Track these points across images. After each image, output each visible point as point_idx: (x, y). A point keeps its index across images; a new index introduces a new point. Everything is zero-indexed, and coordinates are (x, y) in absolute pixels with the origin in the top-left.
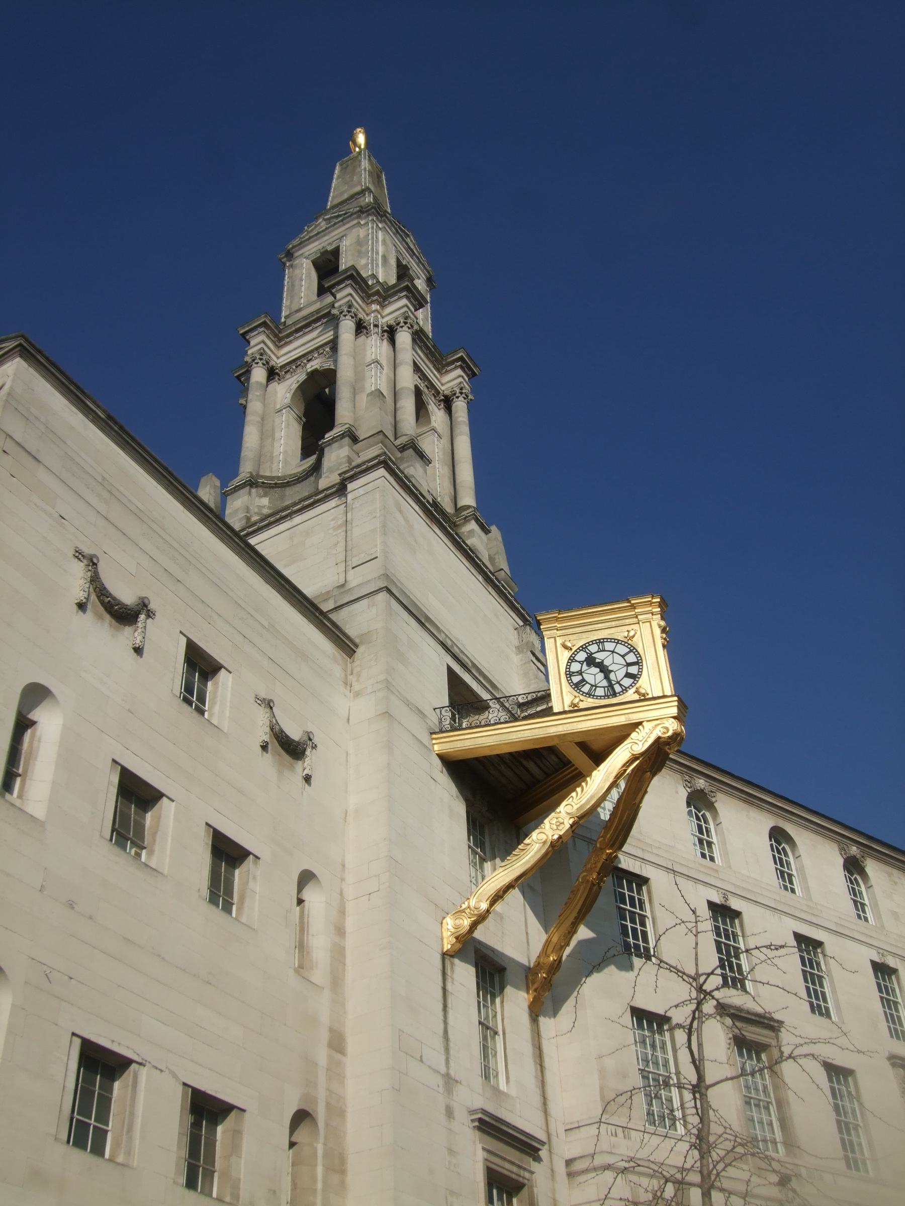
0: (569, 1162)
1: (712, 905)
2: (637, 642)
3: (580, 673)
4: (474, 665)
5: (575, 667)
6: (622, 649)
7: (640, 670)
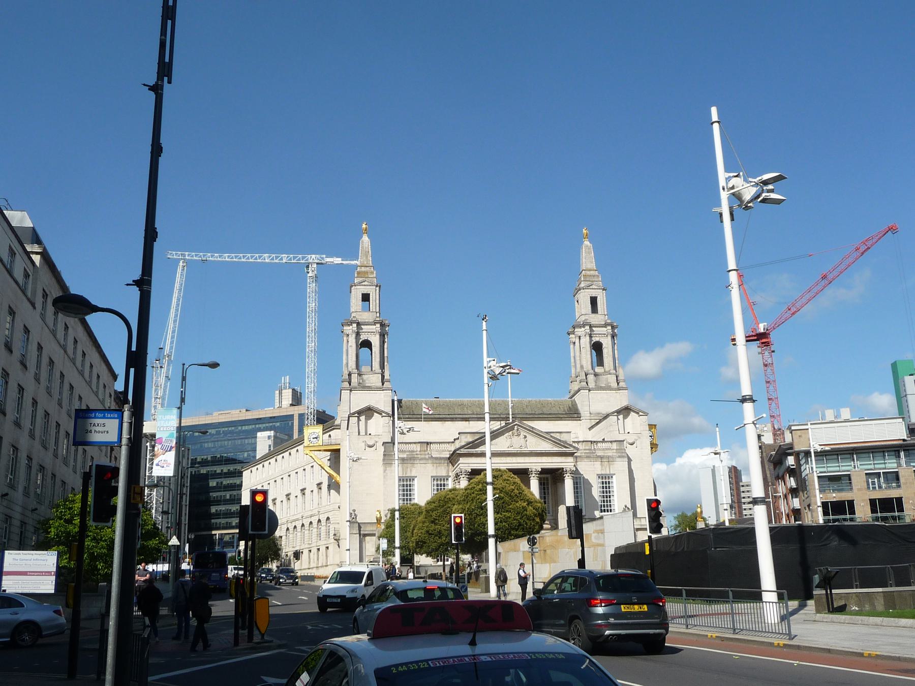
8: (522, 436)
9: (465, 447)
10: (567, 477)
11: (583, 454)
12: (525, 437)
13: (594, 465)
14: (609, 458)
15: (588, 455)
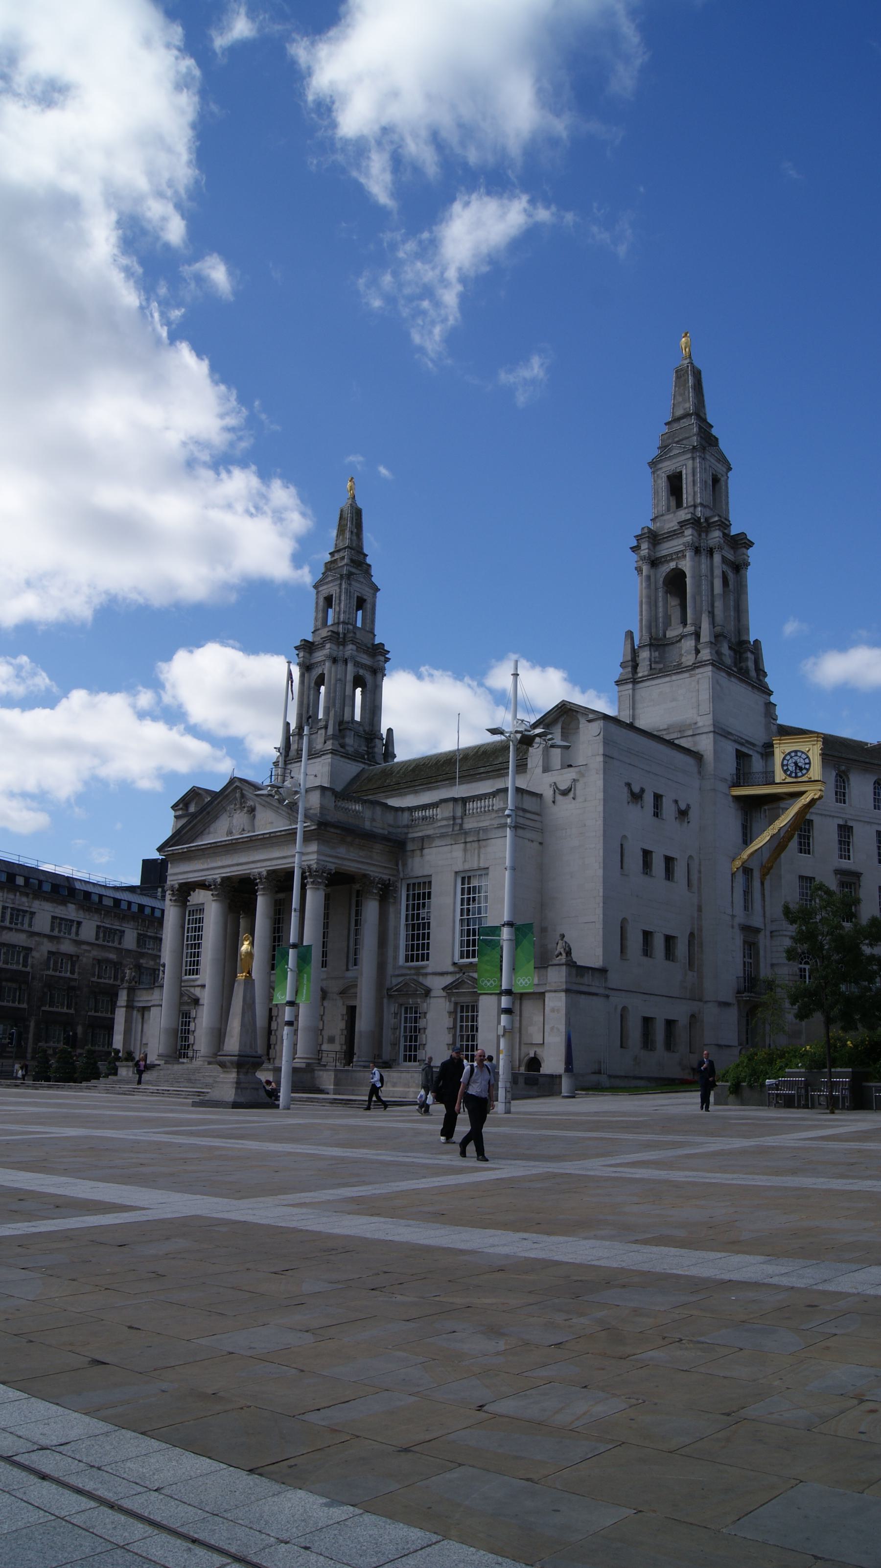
0: (771, 932)
1: (840, 826)
2: (810, 754)
3: (787, 765)
4: (747, 742)
5: (785, 762)
6: (804, 756)
7: (810, 767)
8: (246, 809)
9: (171, 843)
10: (308, 887)
11: (437, 831)
12: (252, 810)
13: (451, 852)
14: (479, 833)
15: (444, 830)
